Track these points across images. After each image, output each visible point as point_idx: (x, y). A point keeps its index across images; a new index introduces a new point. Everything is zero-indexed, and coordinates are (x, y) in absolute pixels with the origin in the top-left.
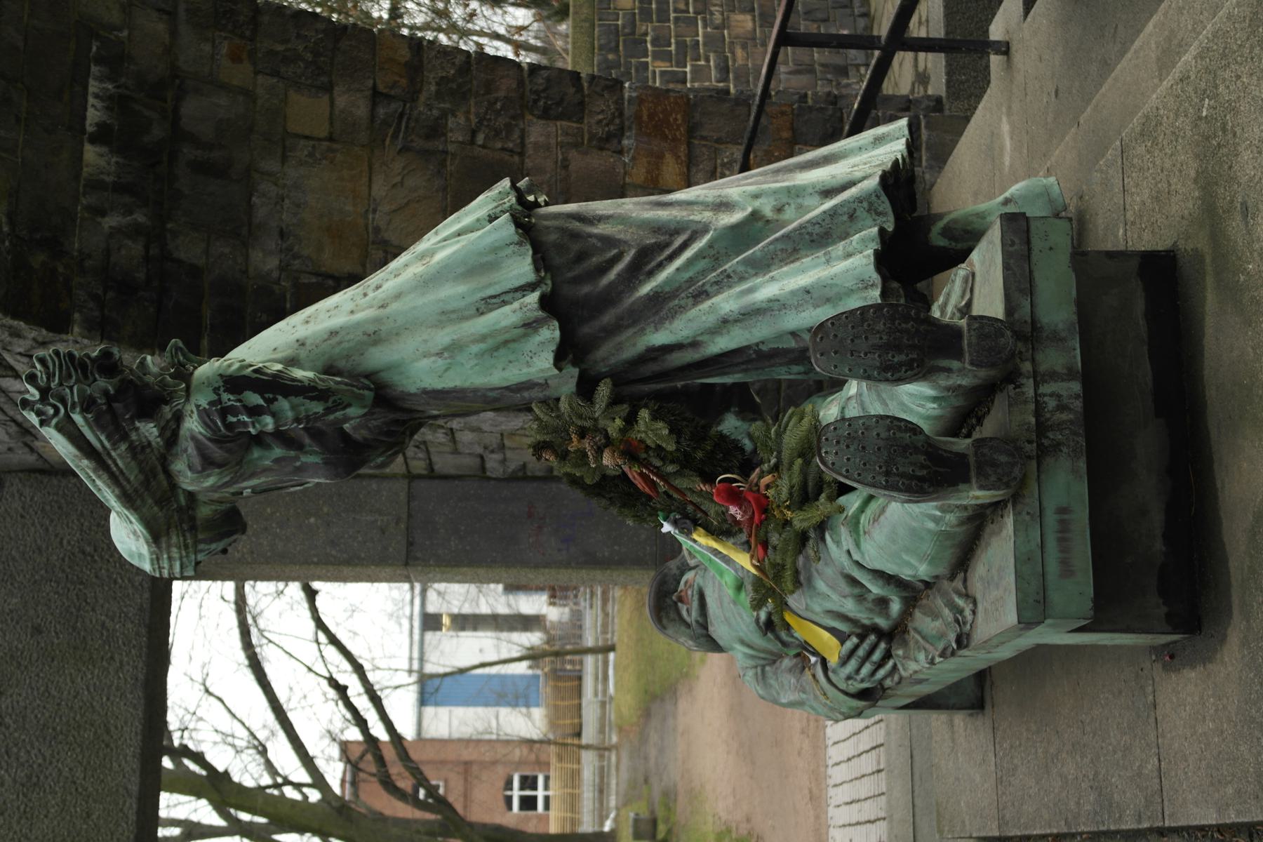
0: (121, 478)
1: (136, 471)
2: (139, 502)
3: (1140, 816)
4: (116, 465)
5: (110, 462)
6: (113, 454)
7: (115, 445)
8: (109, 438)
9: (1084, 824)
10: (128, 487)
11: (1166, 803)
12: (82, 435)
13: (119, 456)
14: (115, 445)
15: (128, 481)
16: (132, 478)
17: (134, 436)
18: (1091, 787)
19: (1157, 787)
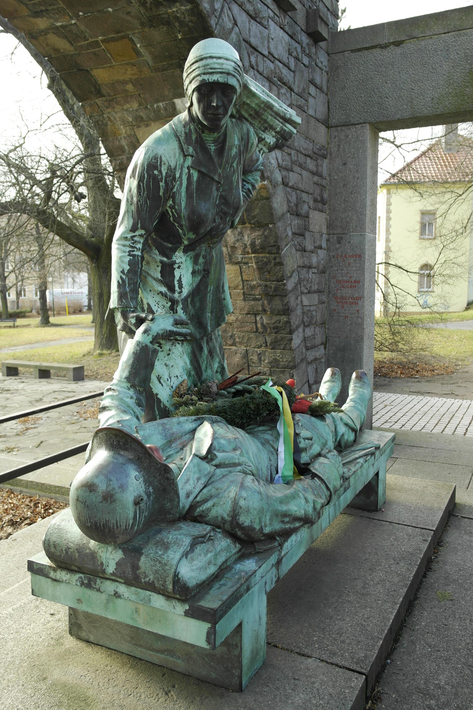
0: (275, 115)
1: (268, 120)
2: (262, 106)
3: (424, 540)
4: (278, 120)
5: (281, 120)
6: (281, 125)
7: (282, 129)
8: (285, 130)
9: (410, 574)
10: (270, 112)
11: (427, 527)
12: (293, 126)
13: (278, 125)
14: (282, 129)
15: (271, 115)
16: (270, 117)
17: (273, 133)
18: (398, 563)
19: (419, 530)
